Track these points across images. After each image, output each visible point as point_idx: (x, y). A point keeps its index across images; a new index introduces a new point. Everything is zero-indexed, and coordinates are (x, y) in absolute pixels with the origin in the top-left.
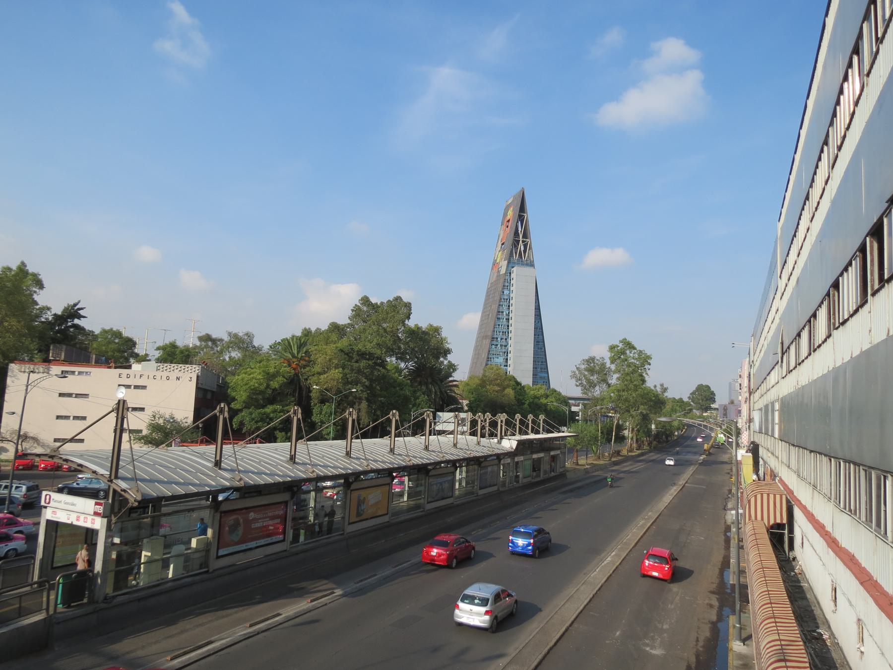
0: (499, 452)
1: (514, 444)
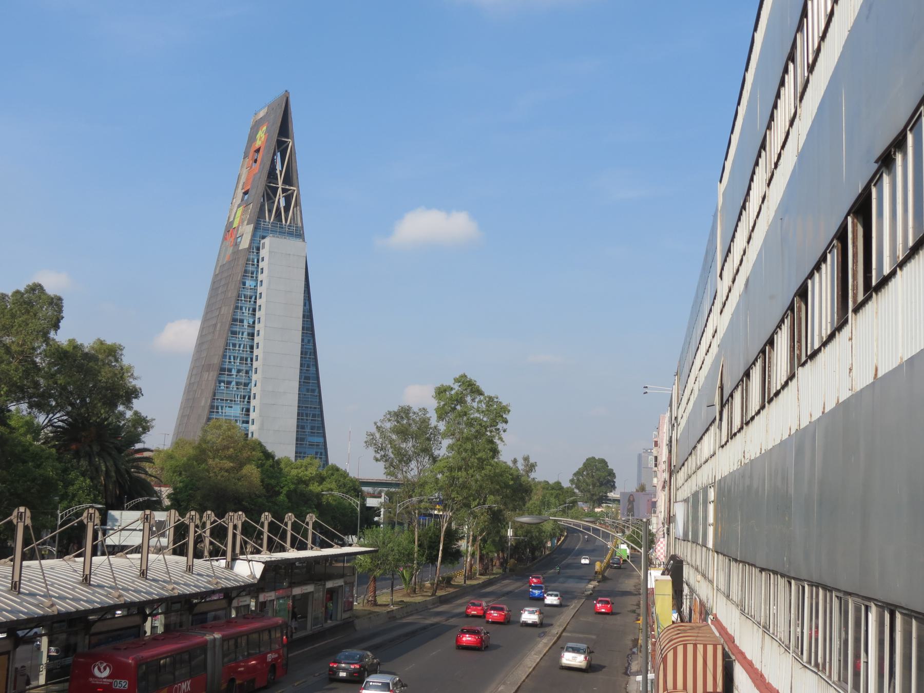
0: (229, 584)
1: (258, 569)
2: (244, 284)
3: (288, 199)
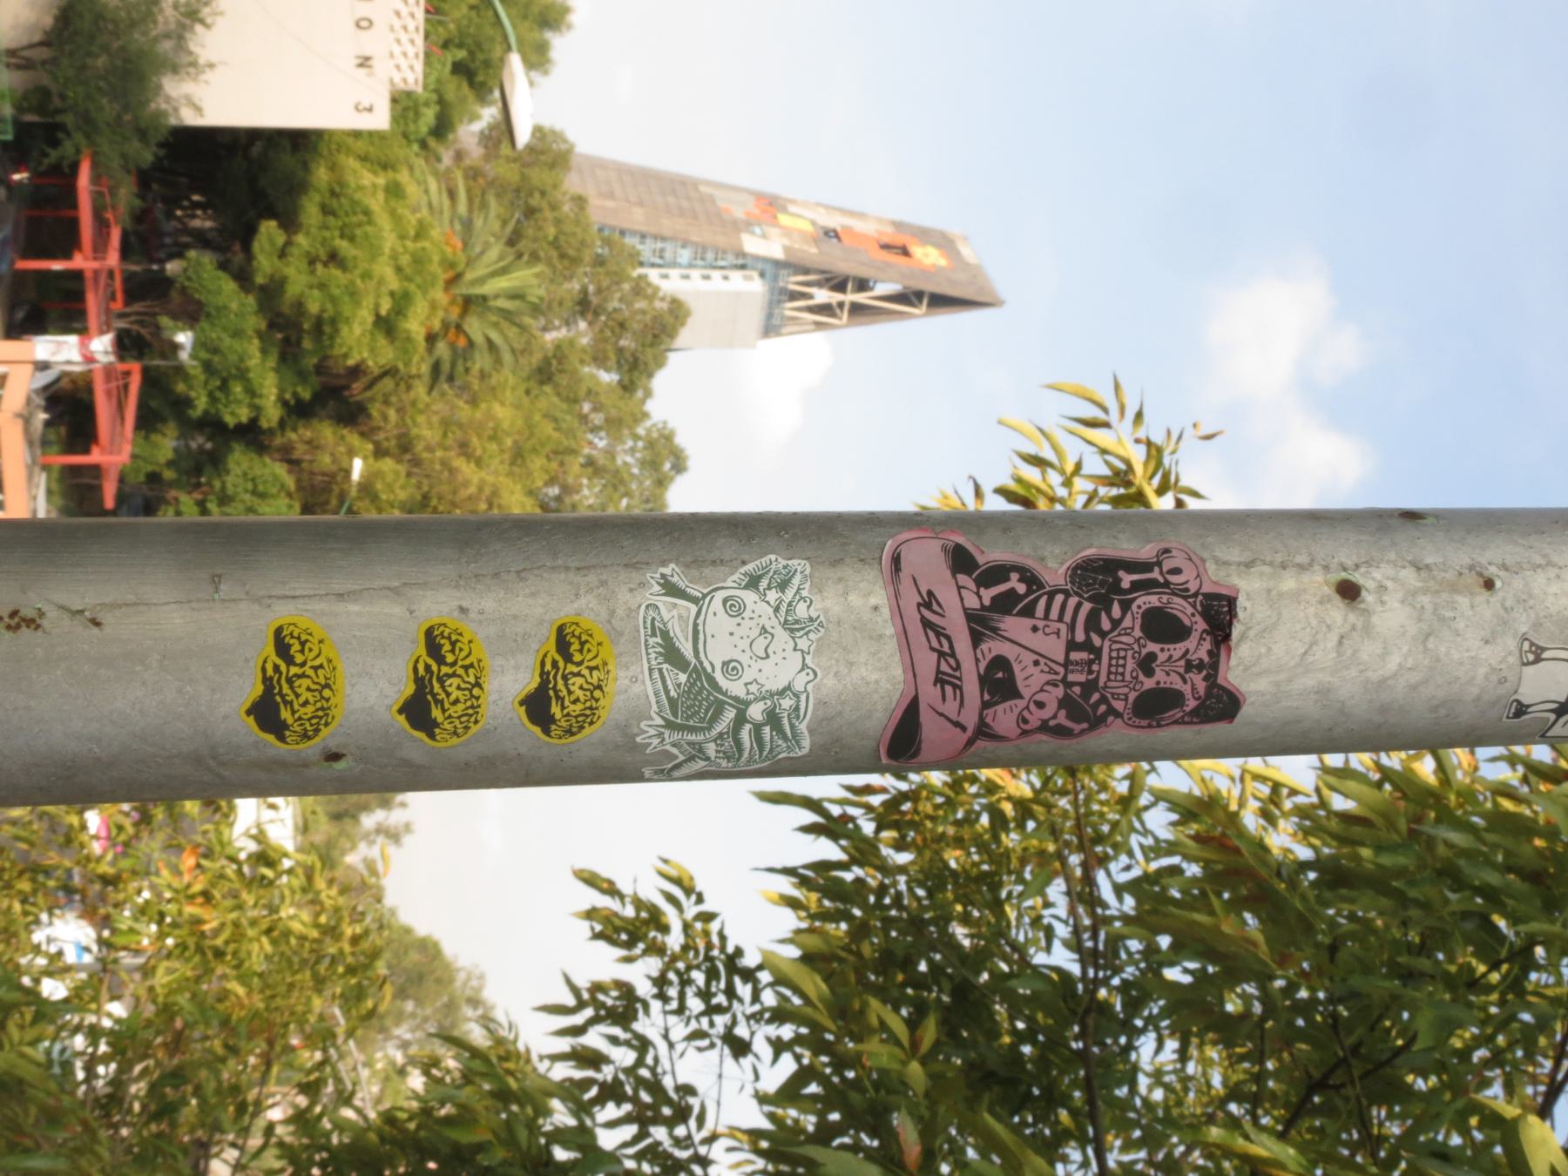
2: (684, 246)
3: (826, 309)
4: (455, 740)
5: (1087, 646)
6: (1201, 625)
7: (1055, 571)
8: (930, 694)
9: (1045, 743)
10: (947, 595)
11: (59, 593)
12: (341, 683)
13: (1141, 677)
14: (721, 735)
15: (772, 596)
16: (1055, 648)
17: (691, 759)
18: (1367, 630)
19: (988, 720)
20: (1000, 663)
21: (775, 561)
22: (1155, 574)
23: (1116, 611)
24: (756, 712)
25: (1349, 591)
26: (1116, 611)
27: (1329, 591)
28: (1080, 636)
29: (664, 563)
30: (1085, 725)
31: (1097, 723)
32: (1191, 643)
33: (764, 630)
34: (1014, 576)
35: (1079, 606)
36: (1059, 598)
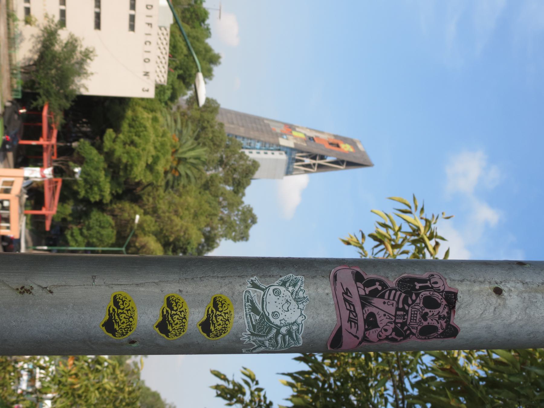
2: (258, 141)
3: (309, 166)
4: (176, 338)
5: (403, 309)
6: (444, 303)
7: (392, 282)
8: (346, 325)
9: (387, 343)
10: (353, 290)
11: (39, 281)
12: (136, 315)
13: (422, 321)
14: (271, 338)
15: (291, 289)
16: (392, 310)
17: (260, 346)
18: (505, 306)
19: (367, 335)
20: (372, 315)
21: (292, 276)
22: (428, 284)
23: (414, 297)
24: (283, 330)
25: (498, 291)
26: (414, 297)
27: (491, 291)
28: (401, 306)
29: (252, 276)
30: (402, 338)
31: (406, 337)
32: (440, 309)
33: (287, 301)
34: (377, 283)
35: (400, 295)
36: (393, 292)
